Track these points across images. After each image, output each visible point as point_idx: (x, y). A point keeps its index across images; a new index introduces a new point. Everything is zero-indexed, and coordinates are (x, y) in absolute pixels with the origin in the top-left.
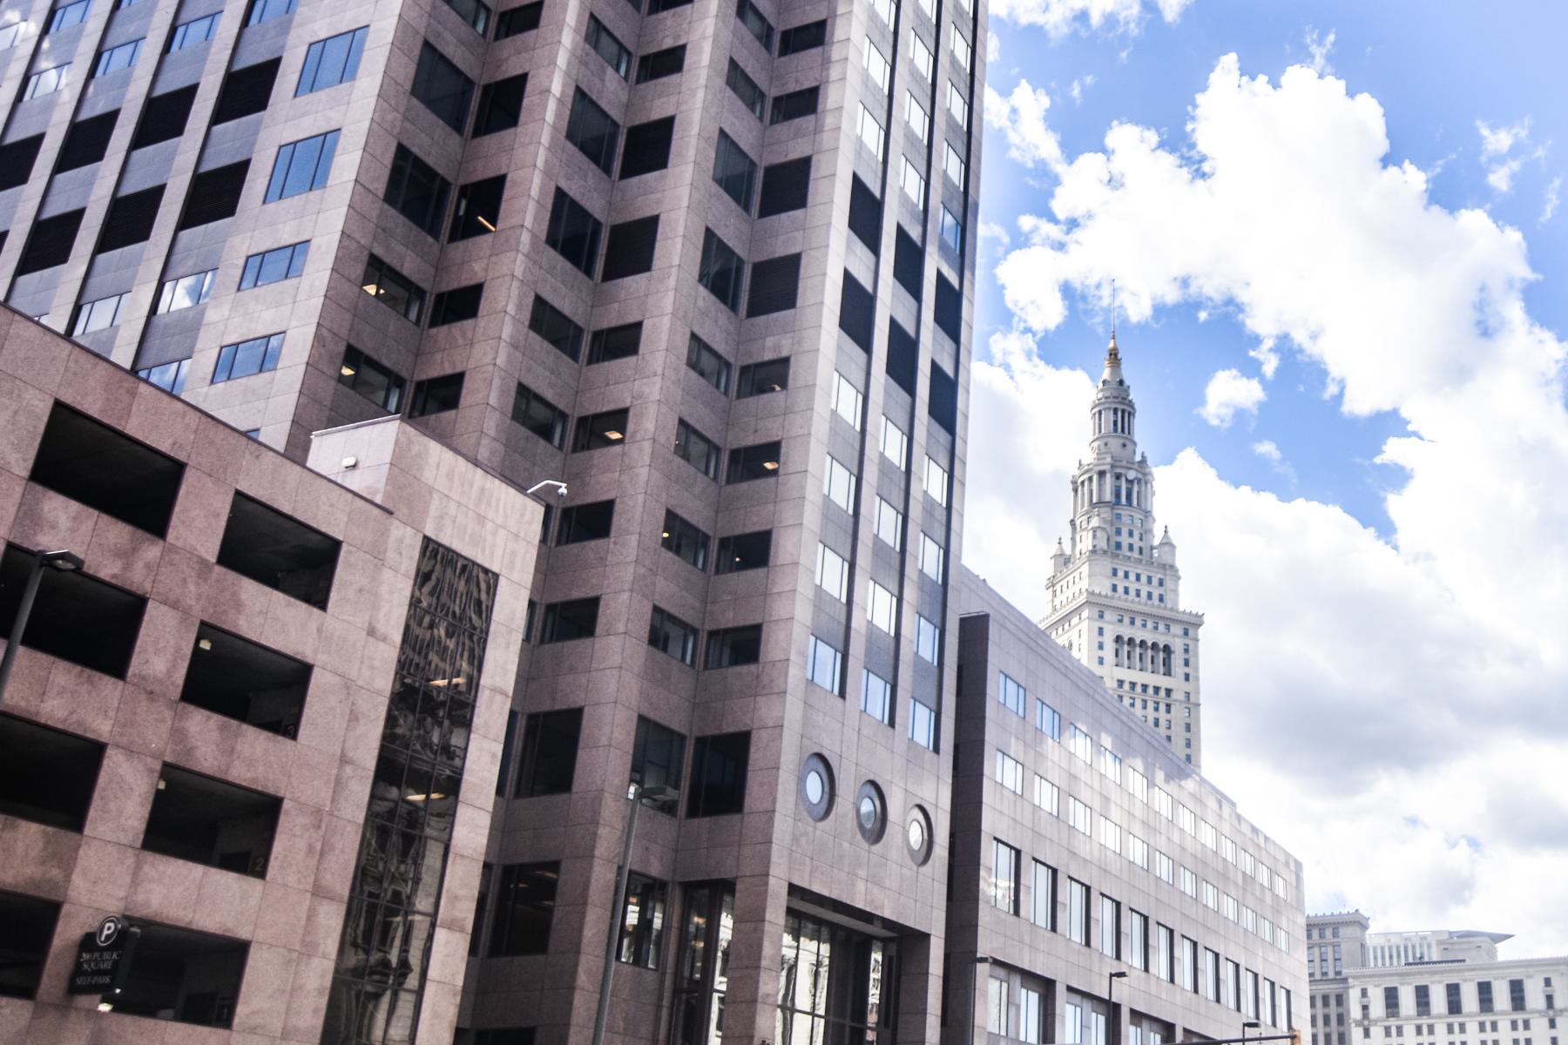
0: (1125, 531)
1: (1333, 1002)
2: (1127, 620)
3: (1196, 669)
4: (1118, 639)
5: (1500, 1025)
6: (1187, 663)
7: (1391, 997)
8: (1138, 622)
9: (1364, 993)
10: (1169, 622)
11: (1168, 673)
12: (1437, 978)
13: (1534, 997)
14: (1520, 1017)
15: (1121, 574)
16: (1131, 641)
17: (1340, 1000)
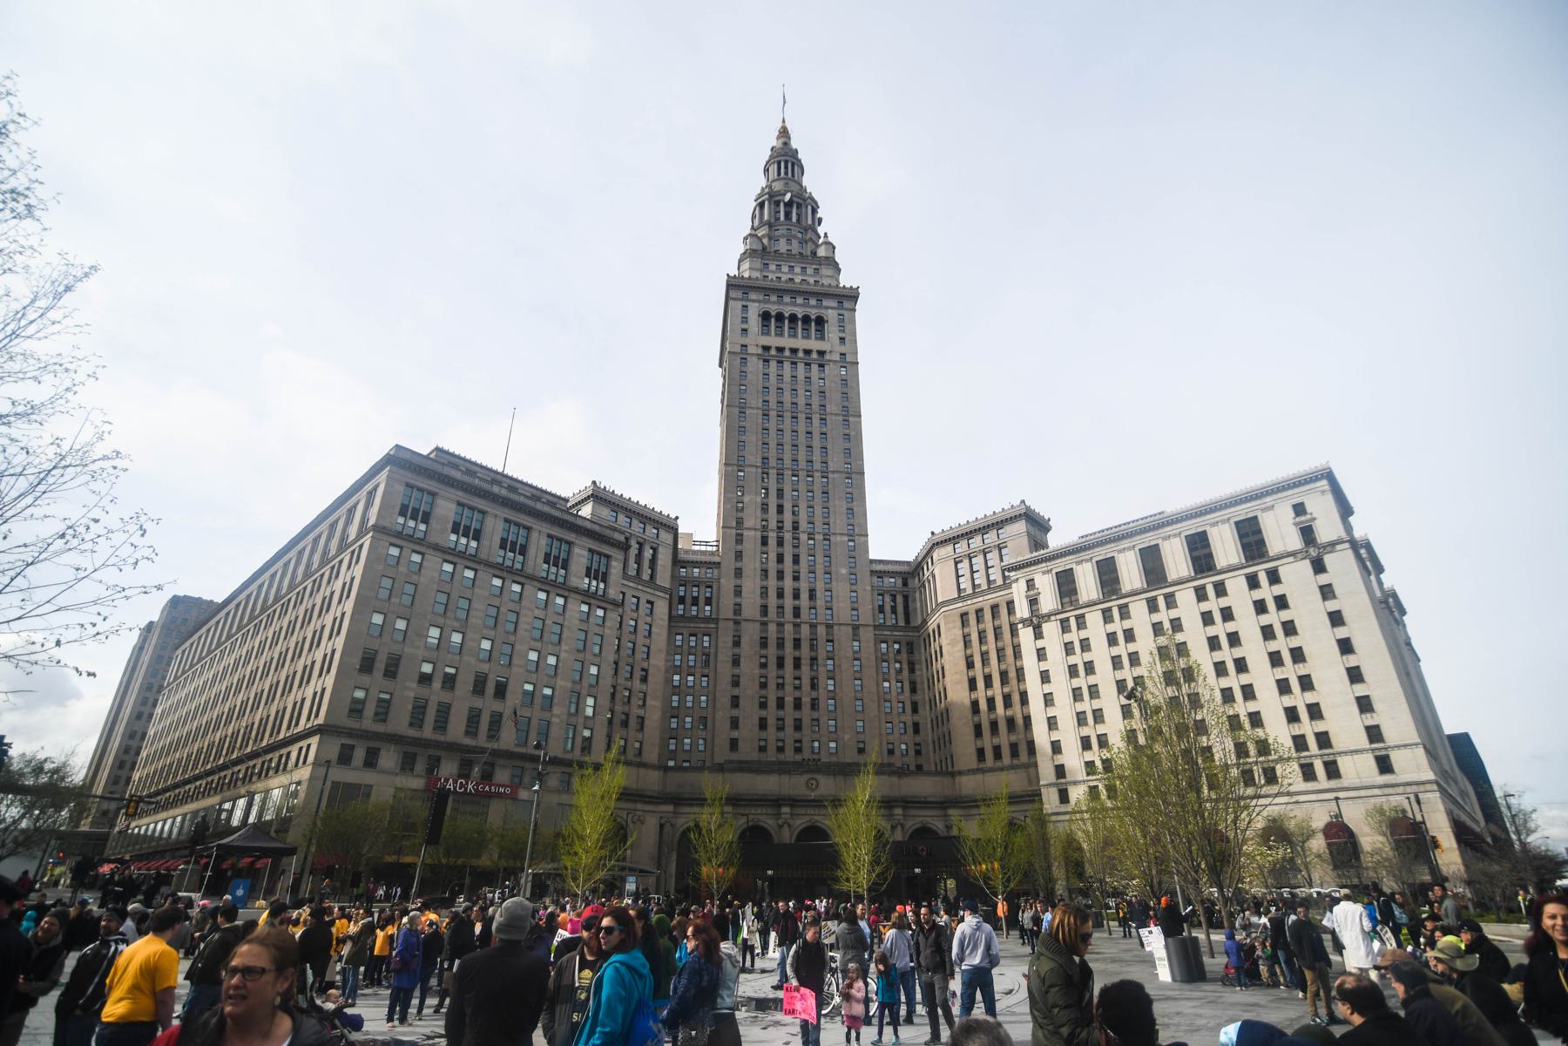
0: (783, 241)
1: (1004, 611)
2: (774, 298)
3: (854, 334)
4: (765, 316)
5: (1229, 585)
6: (842, 328)
7: (1066, 585)
8: (787, 299)
9: (1030, 584)
10: (821, 296)
11: (822, 338)
12: (1125, 544)
13: (1280, 533)
14: (1261, 570)
15: (772, 267)
16: (780, 317)
17: (1010, 605)
